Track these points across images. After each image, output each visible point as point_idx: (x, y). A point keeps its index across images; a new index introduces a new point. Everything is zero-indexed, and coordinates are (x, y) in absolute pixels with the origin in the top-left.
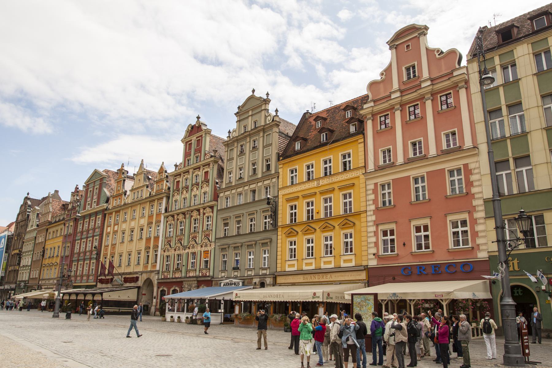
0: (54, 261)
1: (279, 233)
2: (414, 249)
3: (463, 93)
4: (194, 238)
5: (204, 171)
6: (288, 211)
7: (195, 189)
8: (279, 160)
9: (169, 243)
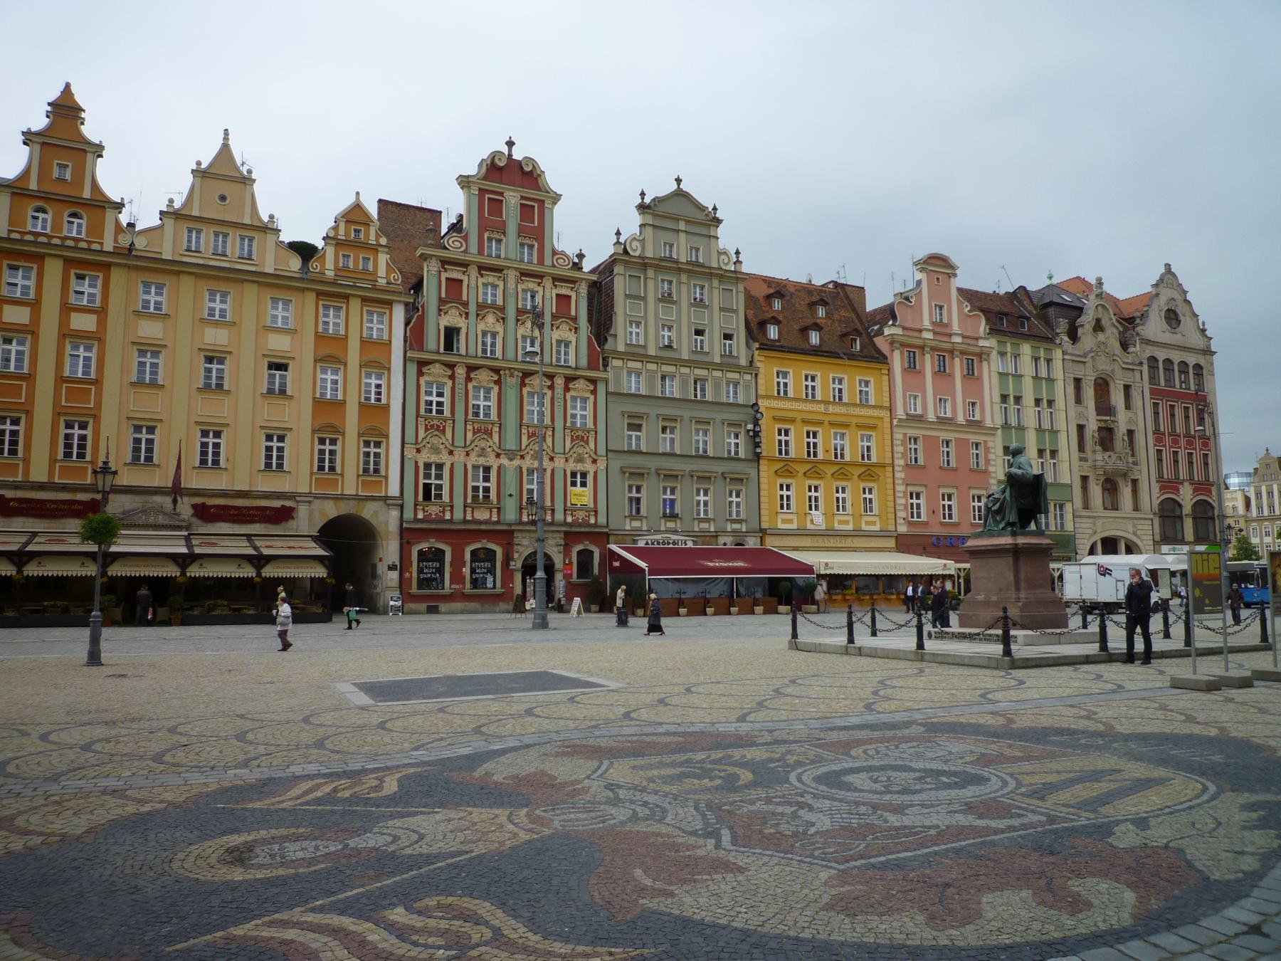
5: (555, 292)
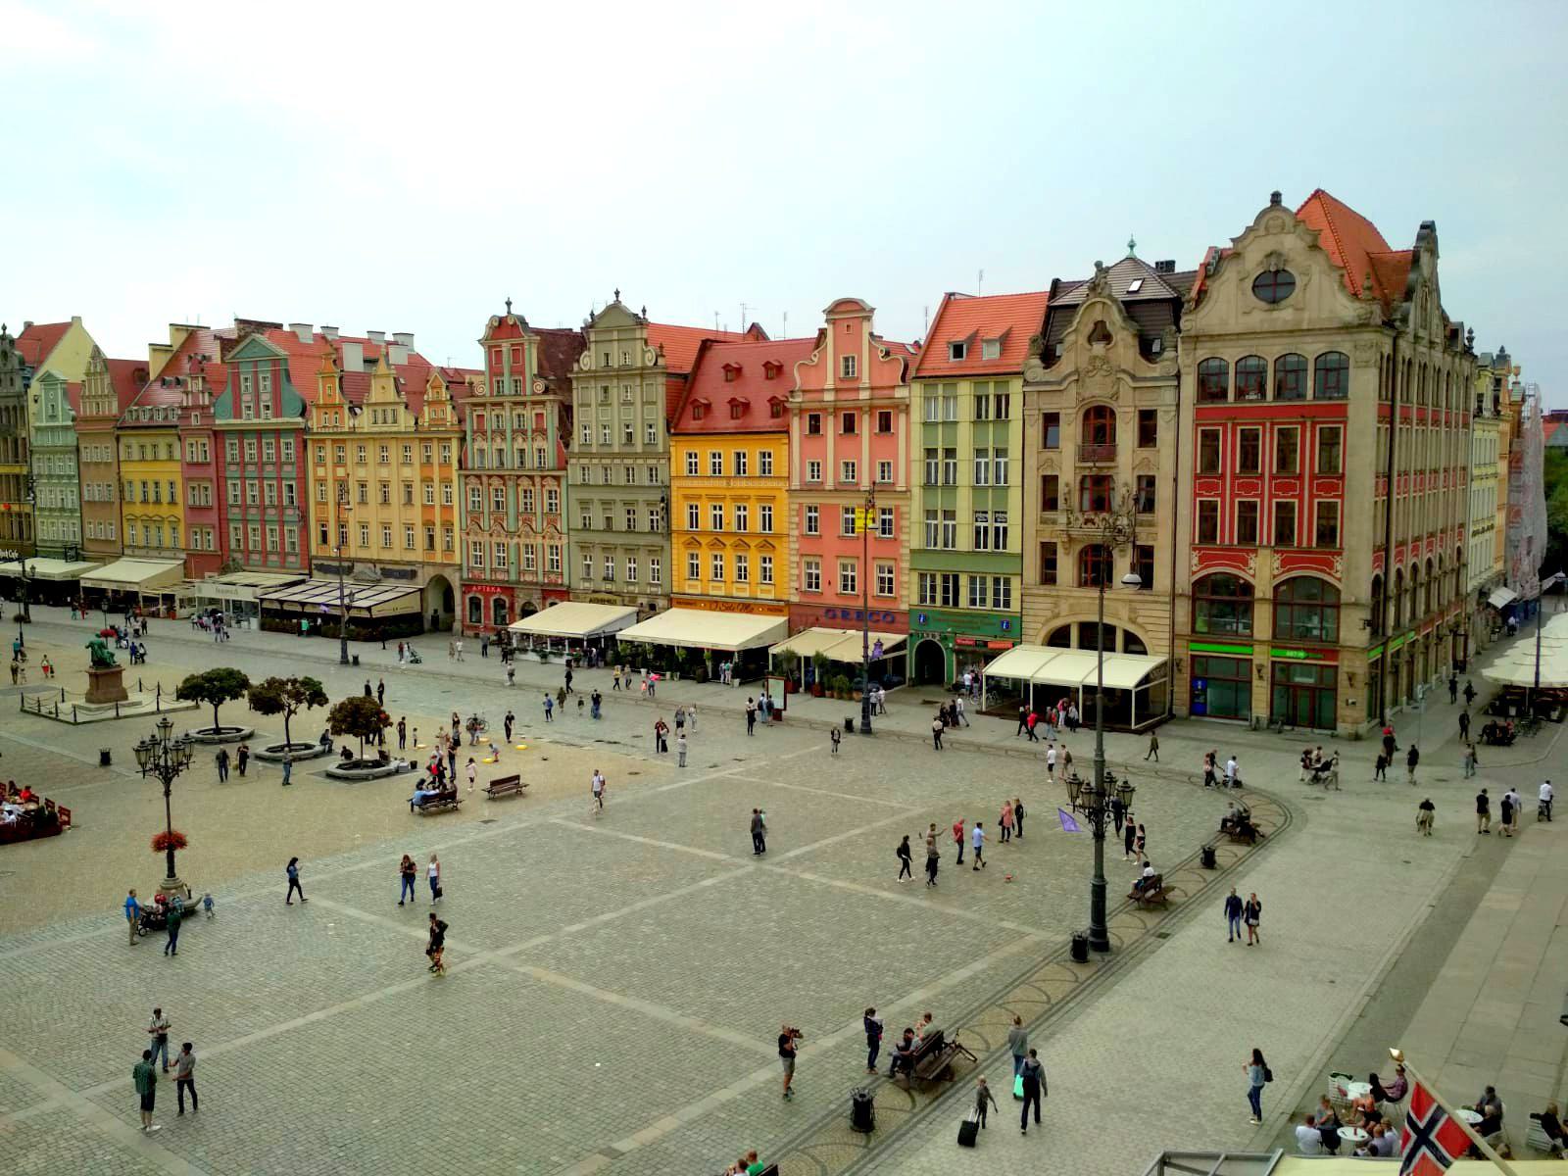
0: (164, 510)
1: (674, 541)
2: (840, 589)
3: (902, 418)
4: (527, 522)
5: (534, 412)
6: (687, 511)
7: (520, 440)
8: (668, 431)
9: (476, 521)
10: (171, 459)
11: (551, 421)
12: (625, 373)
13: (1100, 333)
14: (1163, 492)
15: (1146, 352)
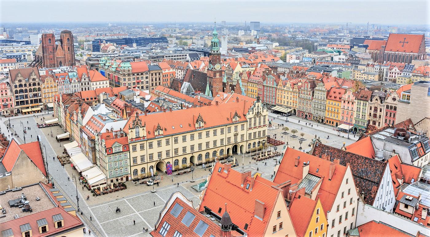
0: (254, 93)
10: (256, 87)
11: (311, 94)
12: (321, 91)
13: (377, 100)
14: (382, 117)
15: (381, 103)
